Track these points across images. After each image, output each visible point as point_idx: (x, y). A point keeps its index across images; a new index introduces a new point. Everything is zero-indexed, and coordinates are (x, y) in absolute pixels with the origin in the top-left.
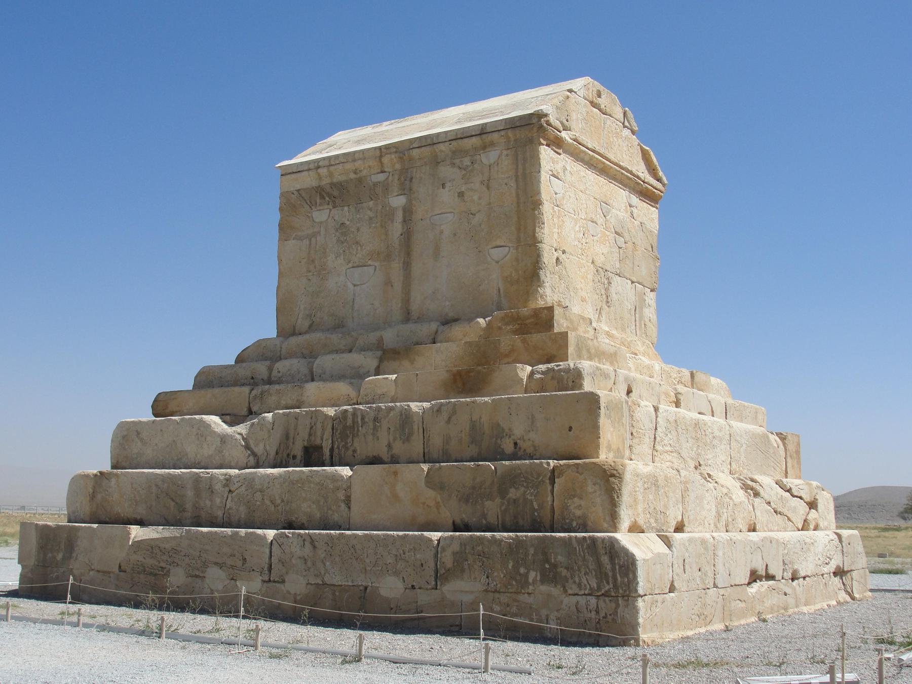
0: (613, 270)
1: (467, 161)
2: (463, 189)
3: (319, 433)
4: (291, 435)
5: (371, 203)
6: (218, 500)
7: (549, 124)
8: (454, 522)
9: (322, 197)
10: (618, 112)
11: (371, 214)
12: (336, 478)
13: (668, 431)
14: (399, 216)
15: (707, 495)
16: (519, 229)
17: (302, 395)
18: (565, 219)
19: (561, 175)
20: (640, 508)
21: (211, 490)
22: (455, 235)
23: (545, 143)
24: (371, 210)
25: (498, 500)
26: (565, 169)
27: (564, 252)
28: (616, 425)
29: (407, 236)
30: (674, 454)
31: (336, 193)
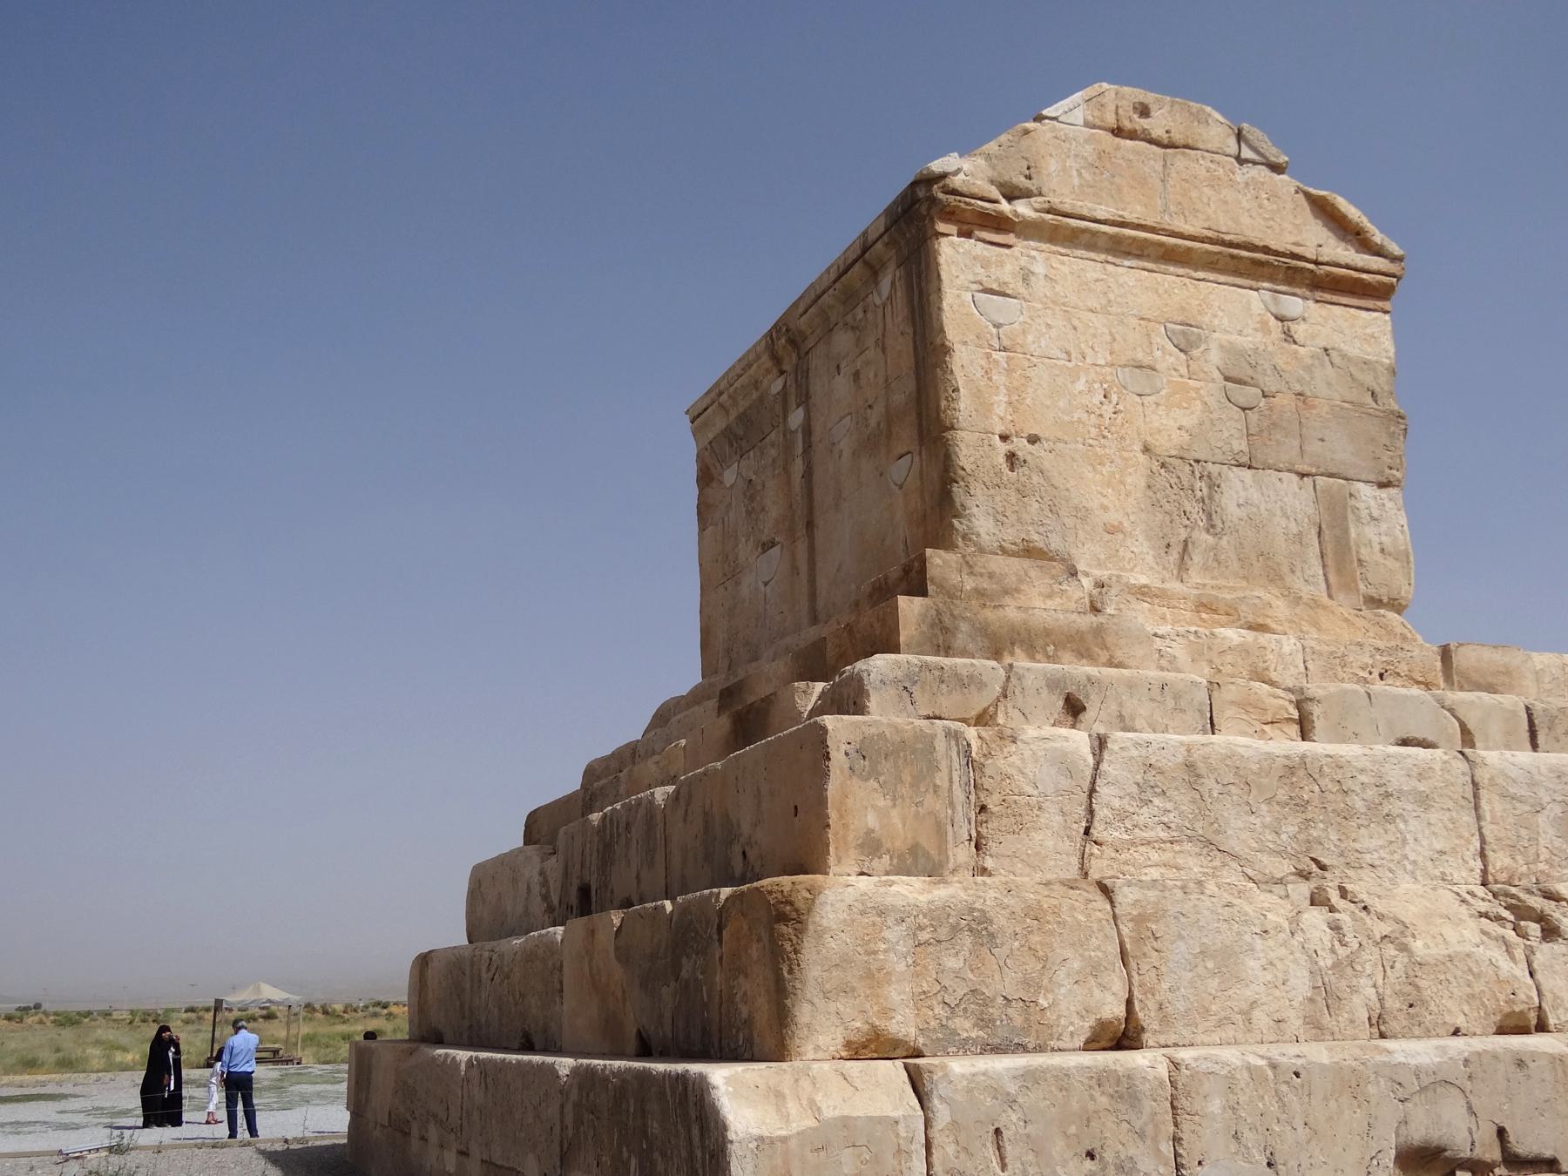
0: (1219, 458)
7: (954, 192)
8: (639, 1032)
10: (1216, 131)
12: (551, 947)
13: (1146, 791)
15: (1259, 943)
18: (1031, 373)
19: (1015, 285)
20: (897, 994)
23: (953, 229)
24: (773, 445)
25: (673, 984)
26: (1026, 276)
27: (1033, 440)
28: (904, 790)
30: (1187, 846)
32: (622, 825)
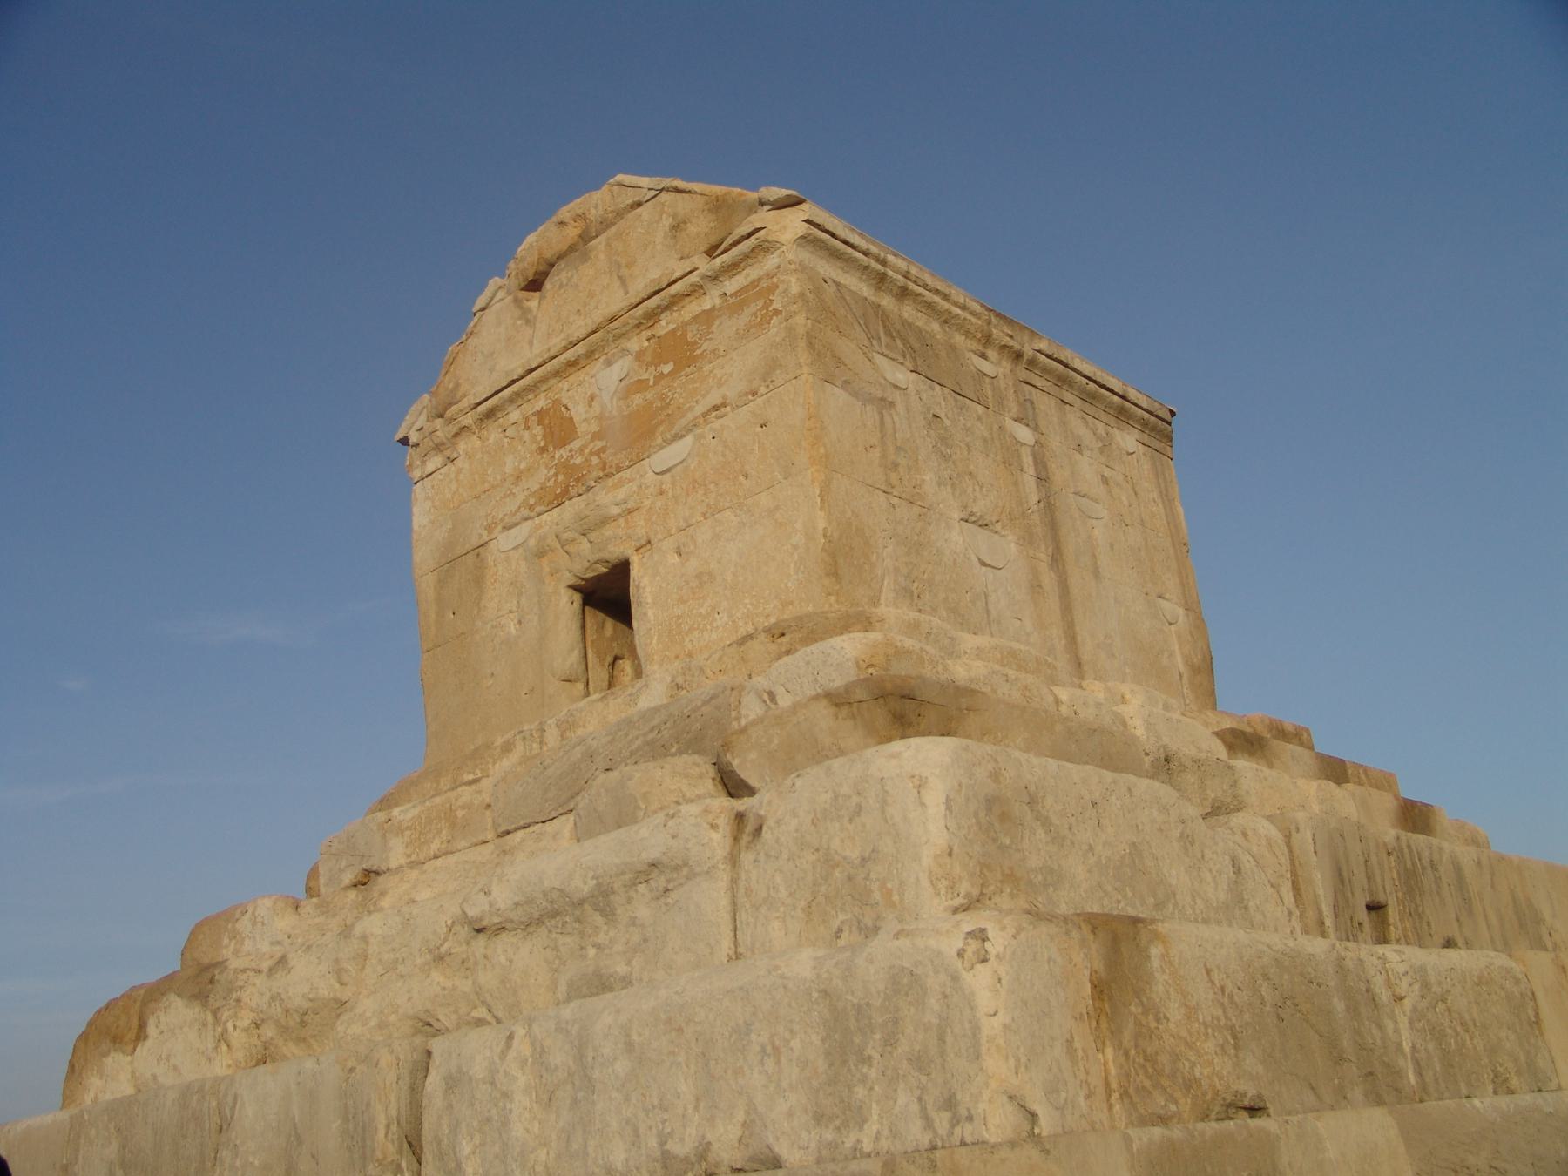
1: (1101, 427)
2: (1107, 472)
3: (1378, 879)
4: (1345, 874)
5: (980, 408)
6: (1390, 1026)
9: (888, 333)
11: (986, 434)
14: (1028, 460)
16: (1182, 585)
17: (1234, 785)
21: (1374, 1001)
22: (1112, 546)
24: (979, 418)
29: (1049, 506)
31: (917, 346)
32: (1426, 861)
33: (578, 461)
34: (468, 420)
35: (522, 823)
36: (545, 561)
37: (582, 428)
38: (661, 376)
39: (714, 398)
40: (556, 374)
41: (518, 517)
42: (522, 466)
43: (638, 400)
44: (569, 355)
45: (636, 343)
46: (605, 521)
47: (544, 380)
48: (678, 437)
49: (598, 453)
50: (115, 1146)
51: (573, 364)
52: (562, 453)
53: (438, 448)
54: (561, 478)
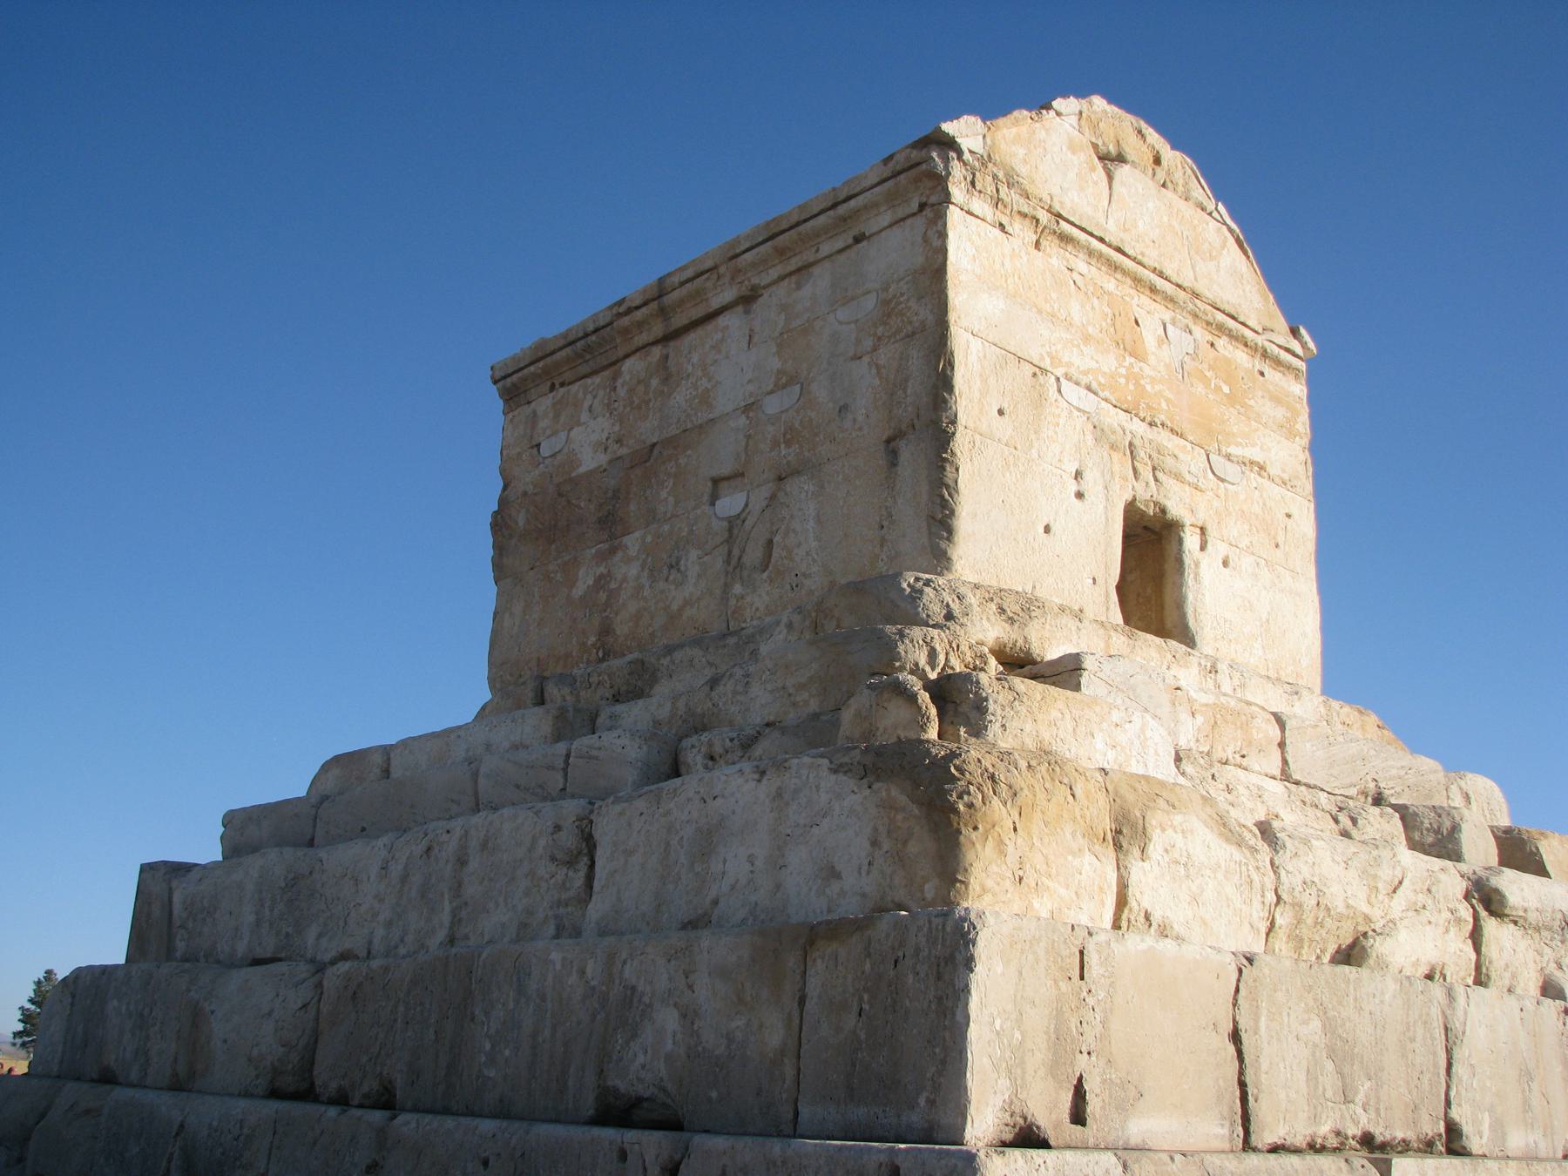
33: (1148, 388)
34: (1044, 217)
35: (1312, 782)
36: (1116, 456)
37: (1152, 359)
38: (1218, 389)
39: (1258, 456)
40: (1137, 281)
41: (1084, 380)
42: (1090, 330)
43: (1200, 389)
44: (1160, 283)
45: (1199, 332)
46: (1178, 477)
47: (1125, 272)
48: (1228, 457)
49: (1168, 401)
50: (1316, 1024)
51: (1153, 290)
52: (1138, 365)
53: (997, 202)
54: (1131, 387)
